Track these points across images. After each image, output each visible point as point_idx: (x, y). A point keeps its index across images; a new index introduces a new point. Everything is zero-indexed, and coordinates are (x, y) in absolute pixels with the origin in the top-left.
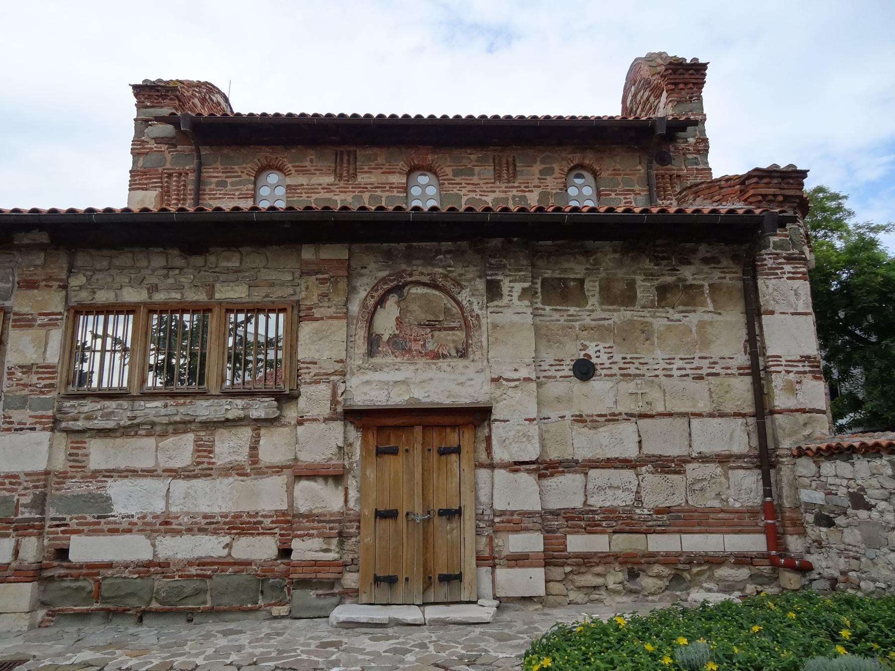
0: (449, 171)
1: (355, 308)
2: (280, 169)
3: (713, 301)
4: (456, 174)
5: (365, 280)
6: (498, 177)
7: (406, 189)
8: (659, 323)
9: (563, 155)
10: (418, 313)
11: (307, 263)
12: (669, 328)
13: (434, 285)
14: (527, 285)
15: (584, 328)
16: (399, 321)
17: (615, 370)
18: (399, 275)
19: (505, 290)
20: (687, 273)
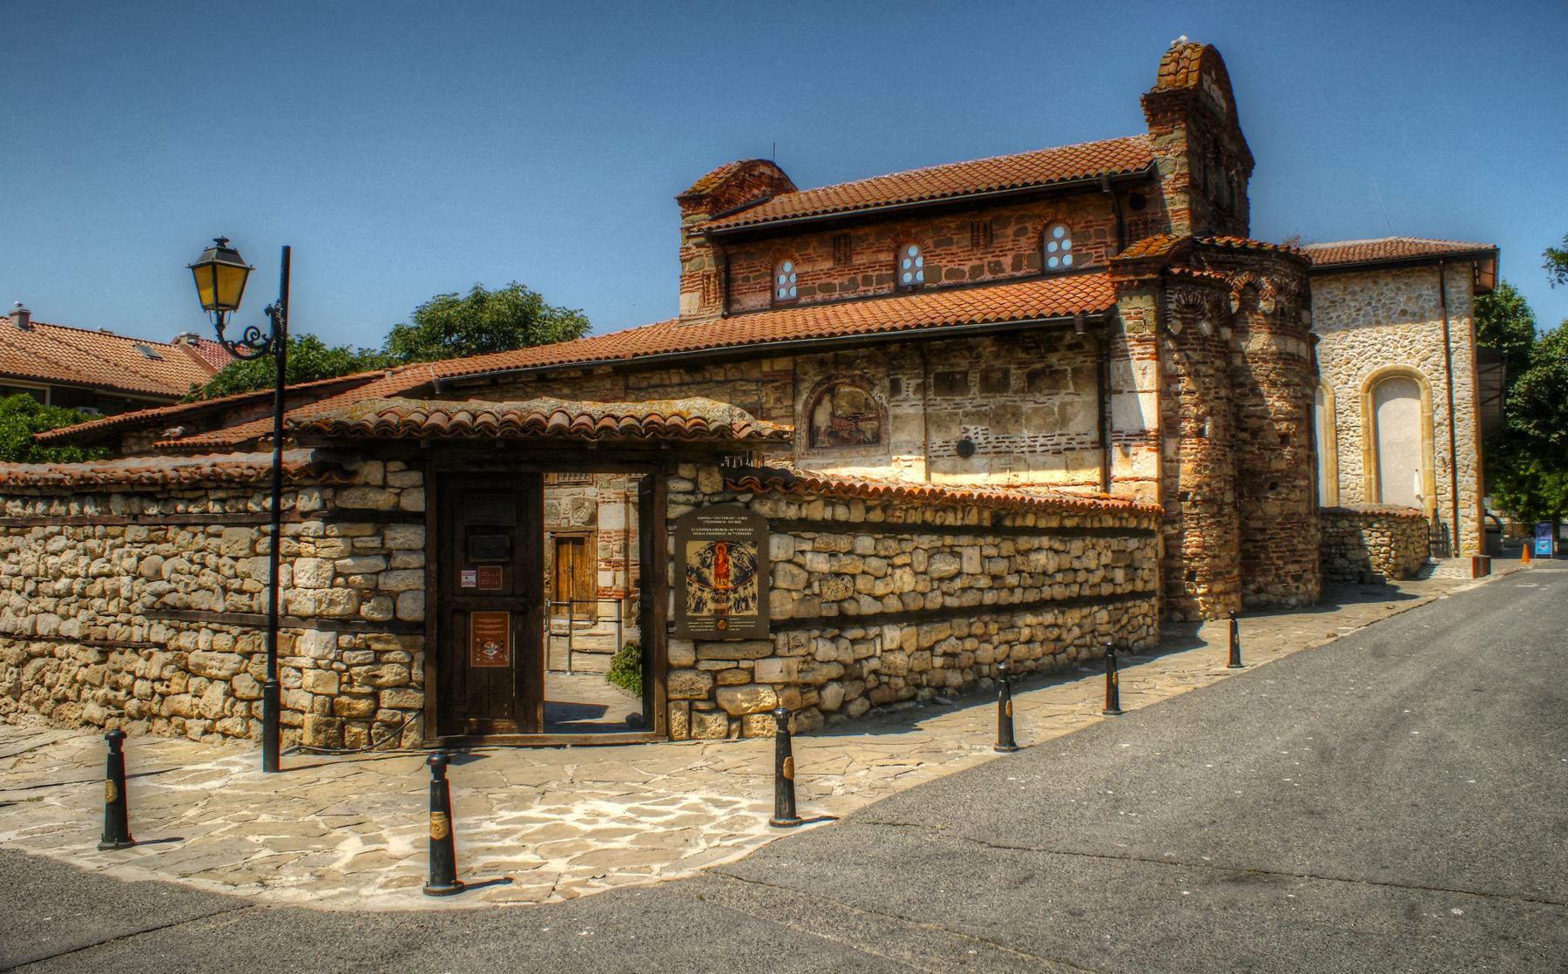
0: (930, 242)
1: (799, 407)
2: (791, 258)
3: (1075, 384)
4: (937, 245)
5: (807, 384)
6: (975, 244)
7: (896, 267)
8: (1027, 407)
9: (1037, 212)
10: (844, 407)
11: (766, 374)
12: (1035, 410)
13: (853, 384)
14: (920, 381)
15: (966, 414)
16: (833, 414)
17: (990, 449)
18: (829, 378)
19: (904, 387)
20: (1053, 359)
